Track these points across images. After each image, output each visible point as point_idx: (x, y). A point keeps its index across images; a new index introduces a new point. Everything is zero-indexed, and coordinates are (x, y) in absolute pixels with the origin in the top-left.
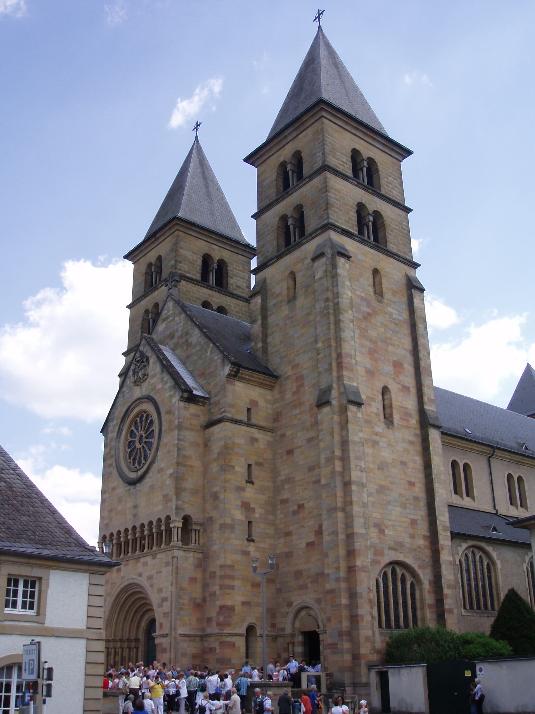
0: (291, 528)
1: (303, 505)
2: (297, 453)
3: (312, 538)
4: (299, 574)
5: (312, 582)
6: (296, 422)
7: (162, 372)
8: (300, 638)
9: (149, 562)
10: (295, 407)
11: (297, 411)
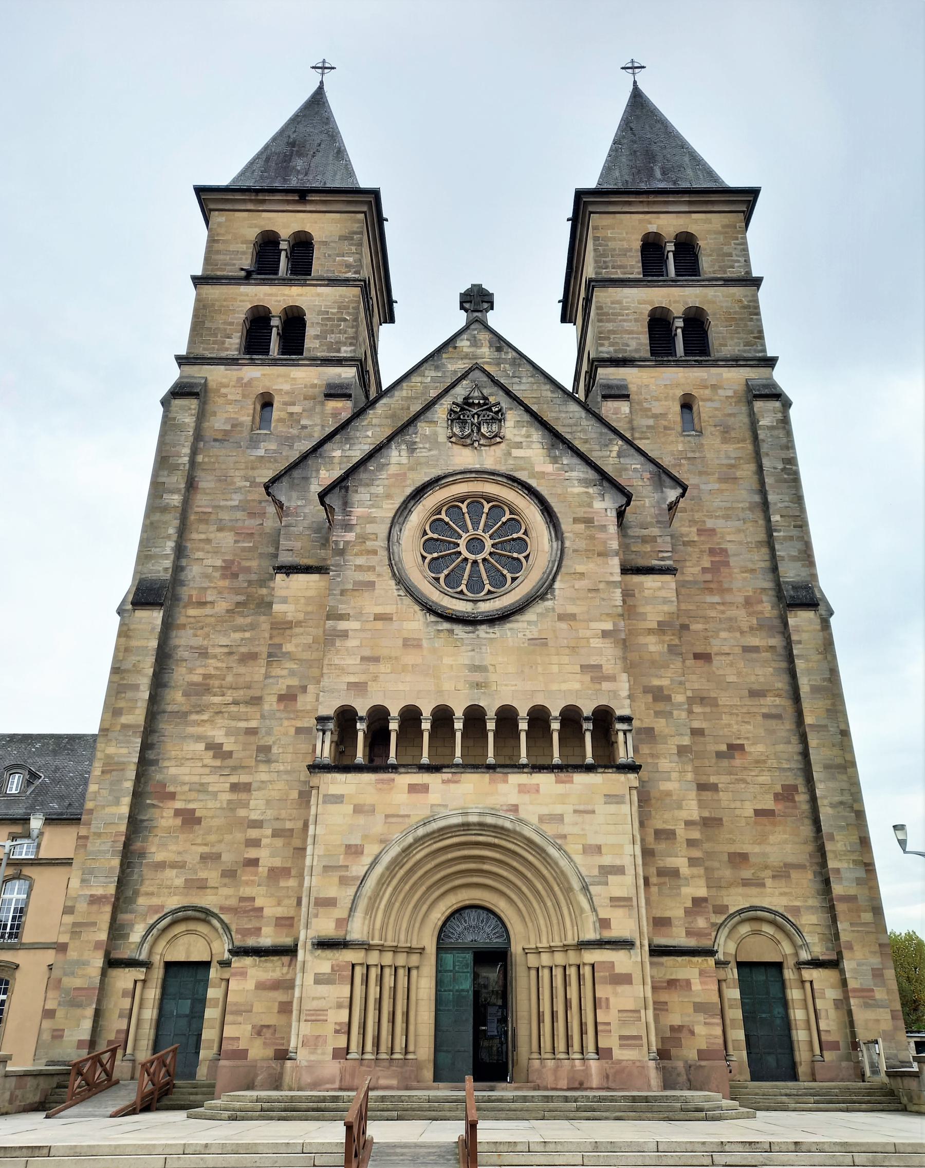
0: (713, 779)
1: (741, 747)
2: (717, 661)
3: (768, 803)
4: (739, 859)
5: (774, 877)
6: (713, 614)
7: (553, 446)
8: (733, 973)
11: (716, 599)
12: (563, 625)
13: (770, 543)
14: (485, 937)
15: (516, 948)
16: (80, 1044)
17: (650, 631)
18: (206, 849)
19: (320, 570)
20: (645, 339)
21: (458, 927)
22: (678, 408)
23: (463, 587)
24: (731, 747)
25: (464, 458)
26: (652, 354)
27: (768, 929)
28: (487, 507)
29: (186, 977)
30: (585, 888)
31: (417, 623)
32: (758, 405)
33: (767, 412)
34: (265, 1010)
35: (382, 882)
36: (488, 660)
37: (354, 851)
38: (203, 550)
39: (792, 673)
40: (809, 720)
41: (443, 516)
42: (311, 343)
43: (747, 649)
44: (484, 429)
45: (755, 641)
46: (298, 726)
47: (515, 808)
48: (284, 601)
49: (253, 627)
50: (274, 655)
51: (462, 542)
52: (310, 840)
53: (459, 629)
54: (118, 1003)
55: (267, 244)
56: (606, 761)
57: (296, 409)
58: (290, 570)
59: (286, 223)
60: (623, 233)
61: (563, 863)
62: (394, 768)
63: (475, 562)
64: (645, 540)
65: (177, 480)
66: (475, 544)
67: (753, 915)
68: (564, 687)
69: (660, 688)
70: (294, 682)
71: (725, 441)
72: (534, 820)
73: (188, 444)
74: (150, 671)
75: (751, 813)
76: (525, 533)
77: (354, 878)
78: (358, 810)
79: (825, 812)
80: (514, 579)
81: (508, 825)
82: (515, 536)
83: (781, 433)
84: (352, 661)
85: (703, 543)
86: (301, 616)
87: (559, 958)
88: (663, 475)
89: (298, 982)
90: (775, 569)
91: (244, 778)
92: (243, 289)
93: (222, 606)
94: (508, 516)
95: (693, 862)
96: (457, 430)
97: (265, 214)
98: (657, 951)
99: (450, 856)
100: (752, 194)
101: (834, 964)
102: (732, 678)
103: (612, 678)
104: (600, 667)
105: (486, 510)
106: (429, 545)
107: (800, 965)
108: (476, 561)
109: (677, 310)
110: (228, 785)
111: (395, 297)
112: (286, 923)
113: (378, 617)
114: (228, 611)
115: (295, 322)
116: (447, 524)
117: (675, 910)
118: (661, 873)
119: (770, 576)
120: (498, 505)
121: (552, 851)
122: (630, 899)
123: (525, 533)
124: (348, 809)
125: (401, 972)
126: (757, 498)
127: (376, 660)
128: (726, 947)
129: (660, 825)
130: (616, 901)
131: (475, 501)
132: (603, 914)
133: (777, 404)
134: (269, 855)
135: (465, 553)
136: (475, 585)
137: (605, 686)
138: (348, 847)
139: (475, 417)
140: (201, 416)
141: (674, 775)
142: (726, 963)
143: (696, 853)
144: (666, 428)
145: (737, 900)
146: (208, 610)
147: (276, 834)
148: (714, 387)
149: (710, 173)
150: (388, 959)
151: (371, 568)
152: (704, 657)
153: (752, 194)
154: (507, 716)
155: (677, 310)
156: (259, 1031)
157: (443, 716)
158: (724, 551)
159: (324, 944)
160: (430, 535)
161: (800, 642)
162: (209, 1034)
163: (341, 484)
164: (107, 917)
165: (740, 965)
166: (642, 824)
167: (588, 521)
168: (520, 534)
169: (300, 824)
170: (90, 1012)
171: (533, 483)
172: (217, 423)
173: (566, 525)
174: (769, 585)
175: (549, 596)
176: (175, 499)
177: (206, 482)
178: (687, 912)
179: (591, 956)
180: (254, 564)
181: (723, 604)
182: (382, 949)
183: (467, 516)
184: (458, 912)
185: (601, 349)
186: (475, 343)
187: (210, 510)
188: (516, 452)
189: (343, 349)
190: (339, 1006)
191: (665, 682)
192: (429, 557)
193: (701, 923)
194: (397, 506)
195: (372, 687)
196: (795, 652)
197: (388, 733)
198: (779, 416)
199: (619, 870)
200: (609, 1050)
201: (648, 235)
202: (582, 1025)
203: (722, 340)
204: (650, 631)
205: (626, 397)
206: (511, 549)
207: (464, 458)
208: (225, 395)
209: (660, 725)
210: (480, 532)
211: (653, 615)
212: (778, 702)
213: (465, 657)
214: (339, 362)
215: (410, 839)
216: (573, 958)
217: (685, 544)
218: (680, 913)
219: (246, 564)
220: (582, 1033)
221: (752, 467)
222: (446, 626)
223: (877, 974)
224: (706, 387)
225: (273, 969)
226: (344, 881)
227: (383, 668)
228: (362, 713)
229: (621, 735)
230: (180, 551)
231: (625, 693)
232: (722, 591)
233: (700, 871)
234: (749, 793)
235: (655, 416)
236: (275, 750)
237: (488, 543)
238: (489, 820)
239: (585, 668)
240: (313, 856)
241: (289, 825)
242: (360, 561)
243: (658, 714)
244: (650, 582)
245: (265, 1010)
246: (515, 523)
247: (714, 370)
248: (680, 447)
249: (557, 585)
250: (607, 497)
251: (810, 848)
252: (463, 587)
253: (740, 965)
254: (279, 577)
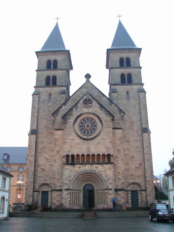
0: (129, 162)
1: (134, 157)
2: (131, 142)
3: (137, 166)
4: (132, 175)
5: (137, 178)
7: (101, 108)
8: (130, 192)
9: (99, 167)
10: (130, 129)
12: (103, 140)
13: (141, 120)
14: (90, 188)
15: (95, 190)
16: (31, 202)
17: (118, 140)
18: (46, 174)
19: (62, 130)
21: (86, 187)
22: (126, 93)
23: (86, 134)
24: (132, 157)
25: (86, 110)
26: (121, 83)
27: (136, 186)
28: (90, 119)
29: (45, 194)
30: (105, 182)
31: (78, 140)
32: (140, 93)
33: (142, 95)
34: (58, 198)
35: (74, 181)
36: (90, 146)
37: (70, 176)
38: (41, 123)
39: (143, 144)
40: (145, 152)
41: (82, 121)
42: (58, 82)
43: (136, 140)
44: (89, 105)
45: (137, 138)
46: (60, 156)
47: (94, 170)
48: (56, 135)
49: (50, 138)
50: (55, 144)
51: (86, 126)
52: (63, 175)
53: (85, 141)
54: (36, 197)
55: (49, 62)
56: (109, 162)
57: (56, 96)
58: (57, 130)
59: (52, 58)
60: (116, 57)
61: (102, 178)
62: (75, 164)
63: (88, 129)
64: (117, 123)
65: (36, 111)
66: (88, 126)
67: (133, 183)
68: (103, 151)
69: (119, 149)
70: (59, 149)
71: (134, 100)
72: (97, 172)
73: (37, 104)
74: (35, 146)
75: (134, 167)
76: (96, 124)
77: (70, 180)
78: (70, 170)
79: (146, 167)
80: (94, 132)
81: (93, 172)
82: (95, 124)
83: (144, 99)
84: (68, 147)
85: (129, 120)
86: (59, 138)
87: (101, 191)
88: (121, 111)
89: (63, 195)
90: (141, 125)
91: (51, 163)
92: (45, 72)
93: (45, 134)
94: (93, 121)
95: (123, 177)
96: (84, 105)
97: (48, 56)
98: (116, 190)
99: (85, 177)
100: (141, 49)
101: (145, 190)
102: (133, 145)
103: (110, 149)
104: (108, 147)
105: (90, 120)
107: (140, 191)
108: (88, 130)
109: (126, 74)
110: (49, 164)
111: (73, 66)
112: (60, 186)
113: (72, 139)
114: (47, 135)
115: (55, 78)
116: (83, 122)
117: (120, 184)
118: (118, 179)
119: (141, 126)
120: (92, 119)
121: (100, 176)
122: (111, 183)
123: (96, 124)
124: (69, 170)
125: (78, 194)
126: (139, 111)
127: (72, 147)
128: (129, 188)
129: (118, 171)
130: (110, 183)
131: (88, 119)
132: (108, 185)
133: (143, 93)
134: (57, 177)
135: (86, 128)
136: (88, 133)
137: (109, 150)
138: (69, 176)
139: (87, 102)
140: (39, 98)
141: (120, 163)
142: (128, 191)
143: (123, 175)
144: (123, 98)
145: (131, 181)
146: (43, 135)
147: (58, 173)
148: (133, 89)
149: (133, 44)
150: (76, 192)
151: (71, 131)
152: (128, 141)
153: (141, 49)
154: (93, 155)
155: (126, 74)
156: (57, 201)
157: (83, 155)
158: (133, 122)
159: (66, 190)
160: (80, 124)
161: (144, 139)
162: (49, 201)
164: (33, 184)
165: (131, 191)
166: (114, 171)
168: (95, 124)
169: (61, 172)
170: (32, 198)
171: (98, 115)
172: (42, 99)
173: (103, 123)
174: (140, 128)
175: (100, 135)
176: (36, 115)
177: (41, 111)
178: (121, 184)
179: (106, 191)
180: (50, 126)
181: (132, 132)
182: (75, 190)
183: (86, 121)
184: (86, 185)
185: (112, 82)
187: (41, 116)
188: (95, 109)
189: (64, 83)
190: (69, 198)
191: (120, 148)
192: (80, 128)
193: (123, 186)
194: (74, 119)
195: (72, 151)
196: (144, 140)
197: (74, 159)
198: (144, 95)
199: (110, 179)
200: (108, 203)
201: (121, 57)
202: (104, 200)
203: (134, 80)
204: (118, 140)
205: (116, 92)
206: (94, 126)
207: (86, 110)
208: (43, 94)
209: (119, 155)
210: (88, 124)
211: (118, 136)
212: (139, 149)
213: (86, 146)
214: (63, 86)
215: (78, 175)
216: (103, 191)
217: (126, 121)
218: (120, 184)
219: (49, 126)
220: (104, 201)
221: (139, 105)
222: (83, 141)
223: (152, 192)
224: (130, 89)
225: (59, 193)
226: (69, 181)
227: (73, 148)
228: (70, 155)
229: (111, 158)
230: (37, 124)
231: (112, 151)
232: (132, 129)
233: (124, 178)
234: (133, 165)
235: (122, 96)
236: (57, 160)
237: (90, 126)
238: (91, 172)
239: (106, 147)
240: (64, 177)
241: (60, 172)
242: (69, 130)
243: (118, 154)
244: (118, 130)
245: (58, 198)
246: (95, 122)
247: (132, 86)
248: (126, 102)
249: (101, 133)
250: (110, 117)
251: (144, 173)
252: (86, 134)
253: (131, 191)
254: (55, 131)
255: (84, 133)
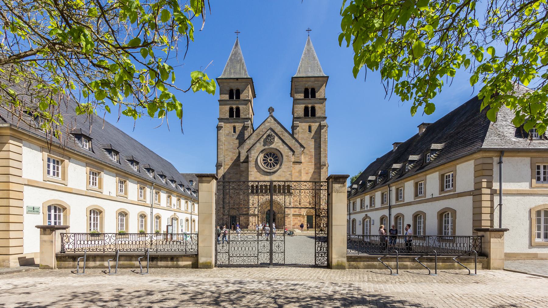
20: (303, 112)
50: (241, 176)
88: (302, 146)
106: (264, 160)
163: (249, 150)
167: (288, 156)
186: (271, 120)
225: (245, 216)
255: (267, 166)
